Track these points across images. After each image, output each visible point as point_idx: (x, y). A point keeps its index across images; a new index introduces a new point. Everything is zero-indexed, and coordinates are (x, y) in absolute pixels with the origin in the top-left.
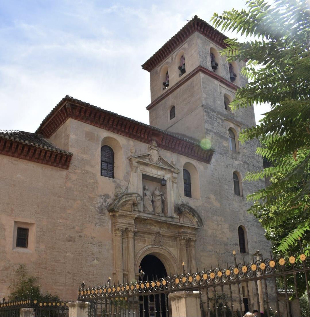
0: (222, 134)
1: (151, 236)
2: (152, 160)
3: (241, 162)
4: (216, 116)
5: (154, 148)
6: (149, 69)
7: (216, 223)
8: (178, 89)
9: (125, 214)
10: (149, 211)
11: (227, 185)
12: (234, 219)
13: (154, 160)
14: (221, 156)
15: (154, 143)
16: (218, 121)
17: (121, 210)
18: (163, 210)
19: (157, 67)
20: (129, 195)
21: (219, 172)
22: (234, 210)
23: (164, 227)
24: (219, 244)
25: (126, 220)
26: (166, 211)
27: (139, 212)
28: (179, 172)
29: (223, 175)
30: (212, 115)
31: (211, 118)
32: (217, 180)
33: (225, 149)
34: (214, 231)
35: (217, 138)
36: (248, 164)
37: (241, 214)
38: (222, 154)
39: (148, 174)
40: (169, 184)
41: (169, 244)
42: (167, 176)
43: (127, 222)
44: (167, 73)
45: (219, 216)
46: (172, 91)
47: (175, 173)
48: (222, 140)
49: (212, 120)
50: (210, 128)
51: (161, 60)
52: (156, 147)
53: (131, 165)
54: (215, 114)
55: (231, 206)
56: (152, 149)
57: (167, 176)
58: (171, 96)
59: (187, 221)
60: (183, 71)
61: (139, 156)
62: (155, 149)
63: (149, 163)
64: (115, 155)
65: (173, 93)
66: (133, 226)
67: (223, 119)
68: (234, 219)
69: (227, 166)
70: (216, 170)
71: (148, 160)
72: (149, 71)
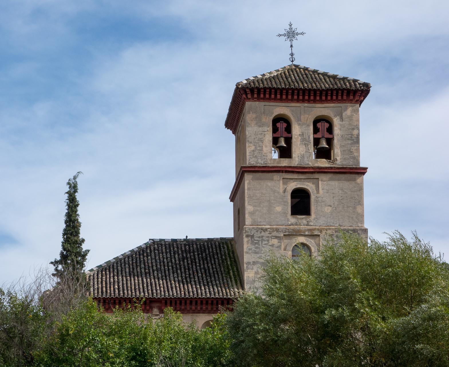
16: (270, 244)
30: (259, 237)
31: (256, 243)
49: (259, 245)
50: (254, 260)
52: (158, 315)
54: (266, 234)
67: (282, 235)
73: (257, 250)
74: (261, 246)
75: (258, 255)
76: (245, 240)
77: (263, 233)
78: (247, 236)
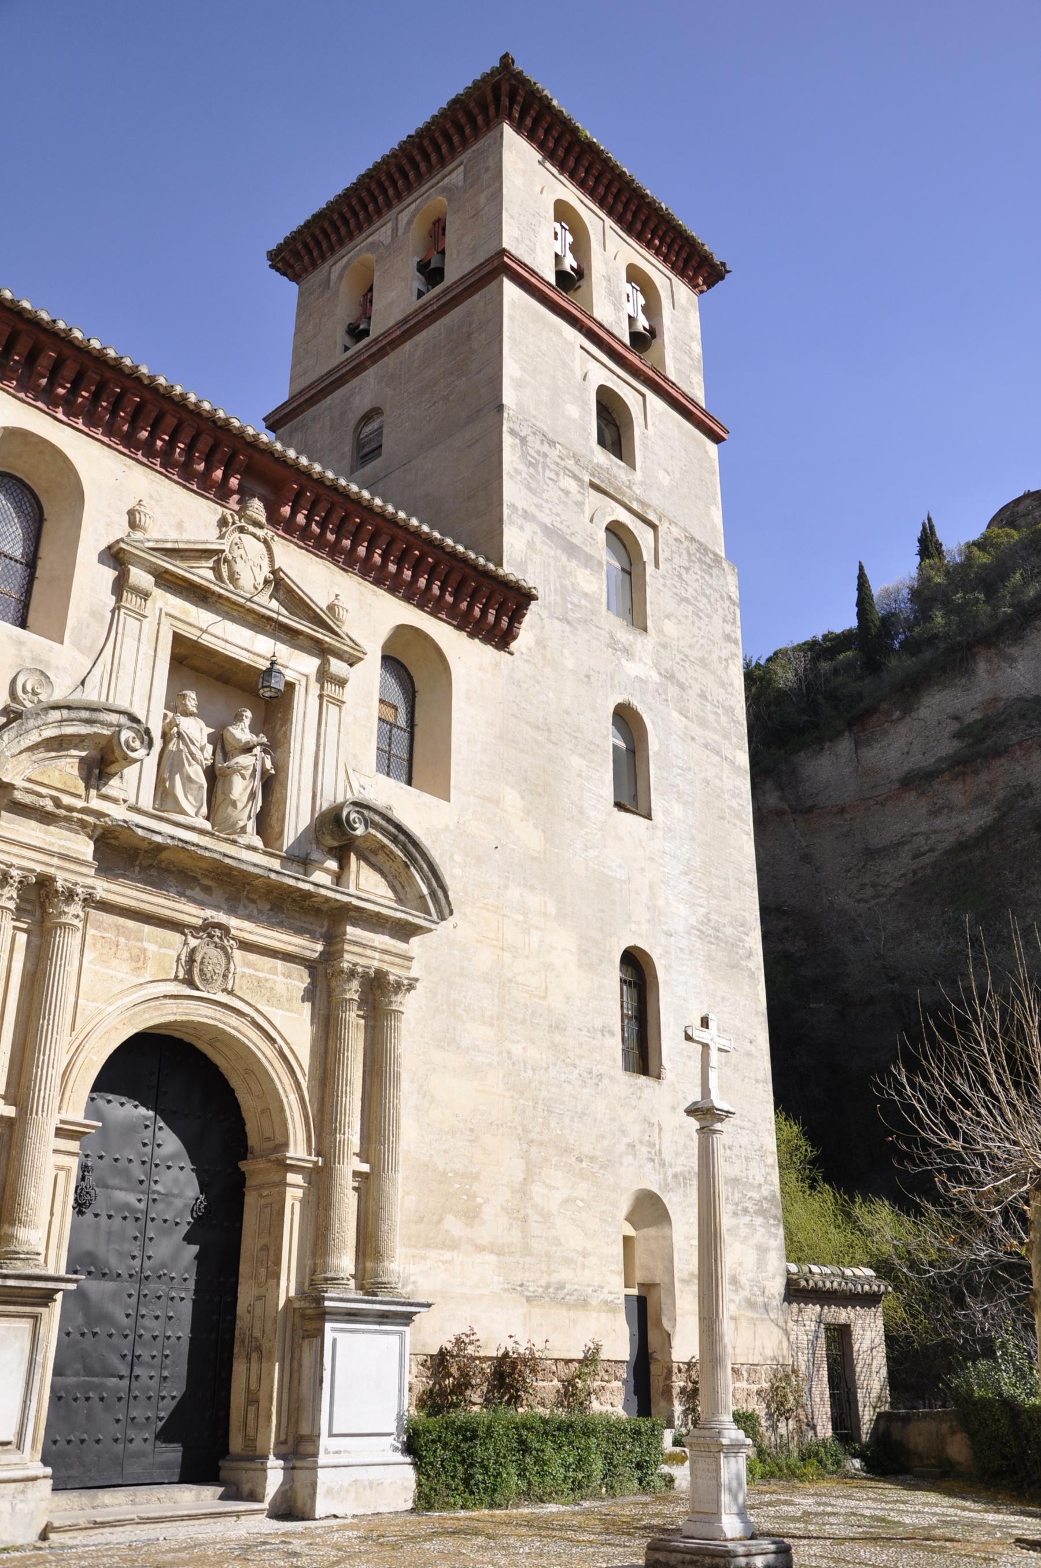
0: (577, 540)
1: (177, 938)
2: (233, 578)
3: (655, 677)
4: (557, 464)
5: (251, 529)
6: (298, 268)
7: (521, 918)
8: (407, 346)
9: (42, 802)
10: (183, 812)
11: (581, 756)
12: (603, 911)
13: (242, 582)
14: (567, 628)
15: (257, 508)
17: (30, 780)
18: (267, 822)
19: (331, 261)
20: (85, 714)
21: (551, 695)
22: (606, 871)
23: (254, 901)
24: (523, 1022)
25: (46, 832)
26: (277, 829)
27: (135, 809)
28: (361, 659)
29: (568, 713)
30: (538, 452)
32: (538, 728)
33: (583, 602)
34: (507, 956)
35: (553, 553)
36: (682, 686)
37: (637, 893)
38: (569, 623)
39: (207, 640)
40: (305, 707)
41: (272, 989)
42: (298, 666)
43: (53, 844)
44: (371, 290)
45: (532, 888)
46: (379, 350)
47: (339, 655)
48: (574, 564)
49: (537, 472)
51: (351, 237)
53: (120, 586)
55: (592, 853)
56: (241, 530)
57: (298, 666)
58: (372, 371)
59: (376, 886)
60: (431, 273)
61: (169, 546)
62: (254, 535)
63: (216, 589)
64: (47, 527)
65: (386, 359)
66: (84, 870)
67: (587, 478)
68: (603, 911)
69: (588, 677)
70: (538, 682)
71: (210, 575)
72: (295, 278)
73: (534, 485)
74: (540, 478)
75: (536, 500)
76: (507, 440)
77: (546, 445)
78: (512, 432)
